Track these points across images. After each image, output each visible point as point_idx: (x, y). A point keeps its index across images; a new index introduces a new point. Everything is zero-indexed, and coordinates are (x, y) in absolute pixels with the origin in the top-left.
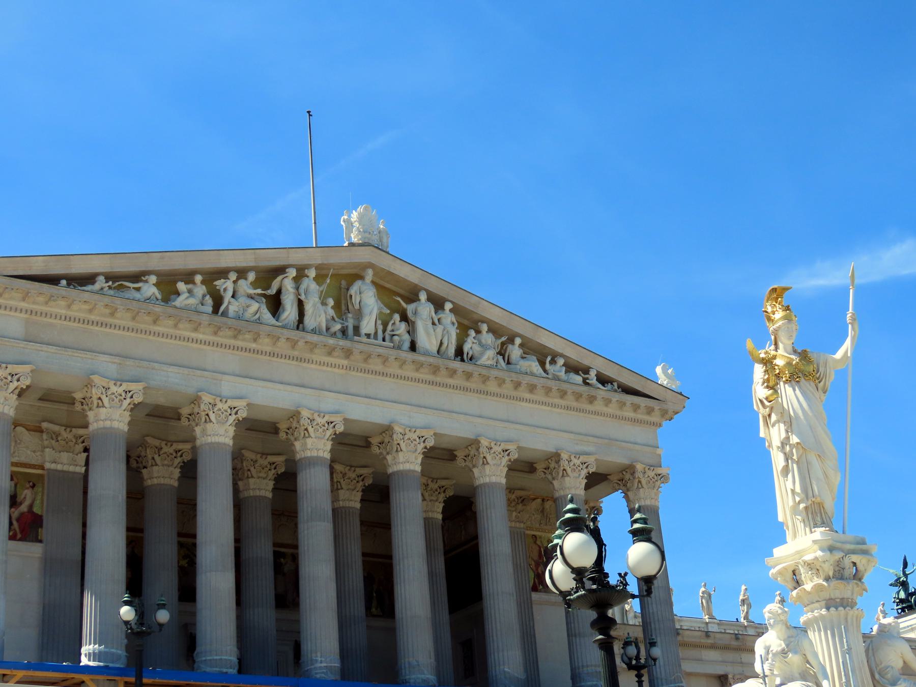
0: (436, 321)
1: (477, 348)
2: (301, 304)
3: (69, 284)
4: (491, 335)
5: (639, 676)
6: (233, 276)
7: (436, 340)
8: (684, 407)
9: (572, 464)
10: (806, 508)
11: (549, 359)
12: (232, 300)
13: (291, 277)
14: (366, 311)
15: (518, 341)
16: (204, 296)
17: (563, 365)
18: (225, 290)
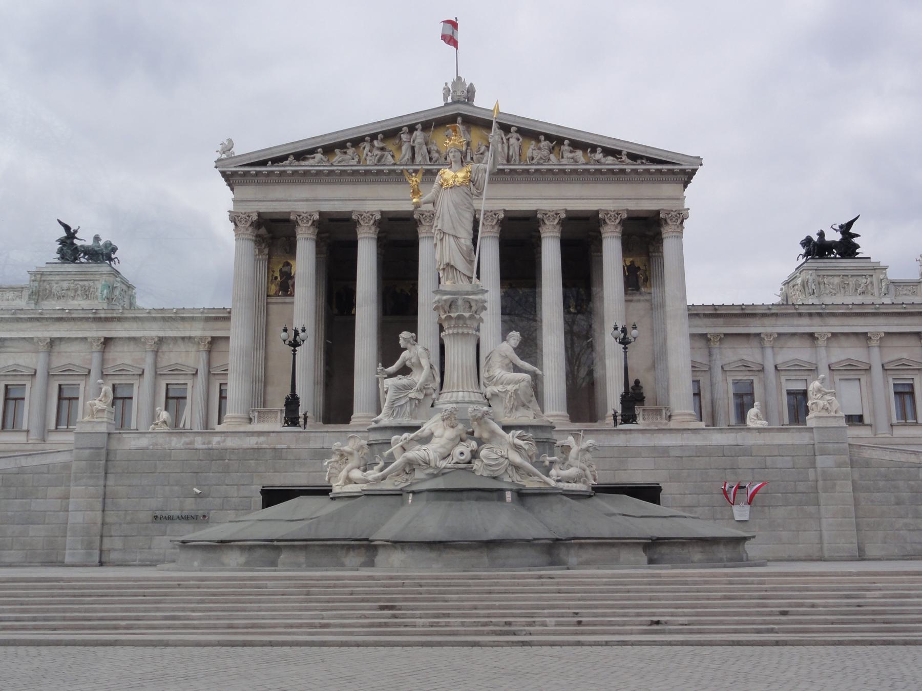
0: (505, 140)
1: (535, 153)
2: (413, 148)
3: (273, 163)
4: (548, 142)
5: (625, 348)
6: (367, 138)
7: (504, 154)
8: (701, 165)
9: (609, 215)
10: (444, 269)
11: (589, 150)
12: (369, 154)
15: (566, 142)
16: (354, 153)
17: (601, 152)
18: (364, 148)
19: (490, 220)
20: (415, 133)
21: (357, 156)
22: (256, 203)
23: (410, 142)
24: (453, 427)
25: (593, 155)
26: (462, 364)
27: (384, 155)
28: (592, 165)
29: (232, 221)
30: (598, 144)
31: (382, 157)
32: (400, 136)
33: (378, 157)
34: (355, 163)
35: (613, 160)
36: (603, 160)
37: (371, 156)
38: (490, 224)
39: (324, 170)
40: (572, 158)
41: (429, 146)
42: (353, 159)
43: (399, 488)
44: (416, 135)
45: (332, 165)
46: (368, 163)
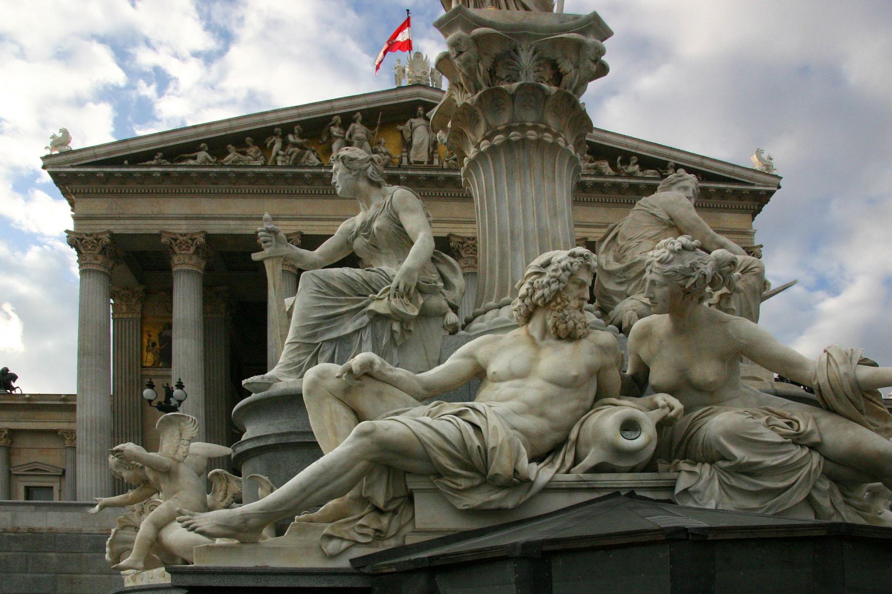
11: (619, 158)
12: (281, 152)
13: (338, 124)
14: (415, 141)
16: (256, 153)
18: (273, 144)
19: (471, 250)
20: (352, 125)
21: (262, 157)
22: (108, 222)
23: (343, 138)
24: (571, 337)
25: (623, 167)
26: (541, 230)
27: (304, 154)
28: (624, 177)
29: (72, 246)
30: (633, 151)
31: (300, 156)
32: (329, 131)
33: (293, 157)
34: (260, 164)
35: (655, 174)
36: (640, 174)
37: (284, 156)
38: (471, 255)
39: (209, 172)
40: (595, 168)
41: (374, 147)
42: (256, 160)
43: (343, 563)
44: (354, 129)
45: (222, 165)
46: (279, 164)
